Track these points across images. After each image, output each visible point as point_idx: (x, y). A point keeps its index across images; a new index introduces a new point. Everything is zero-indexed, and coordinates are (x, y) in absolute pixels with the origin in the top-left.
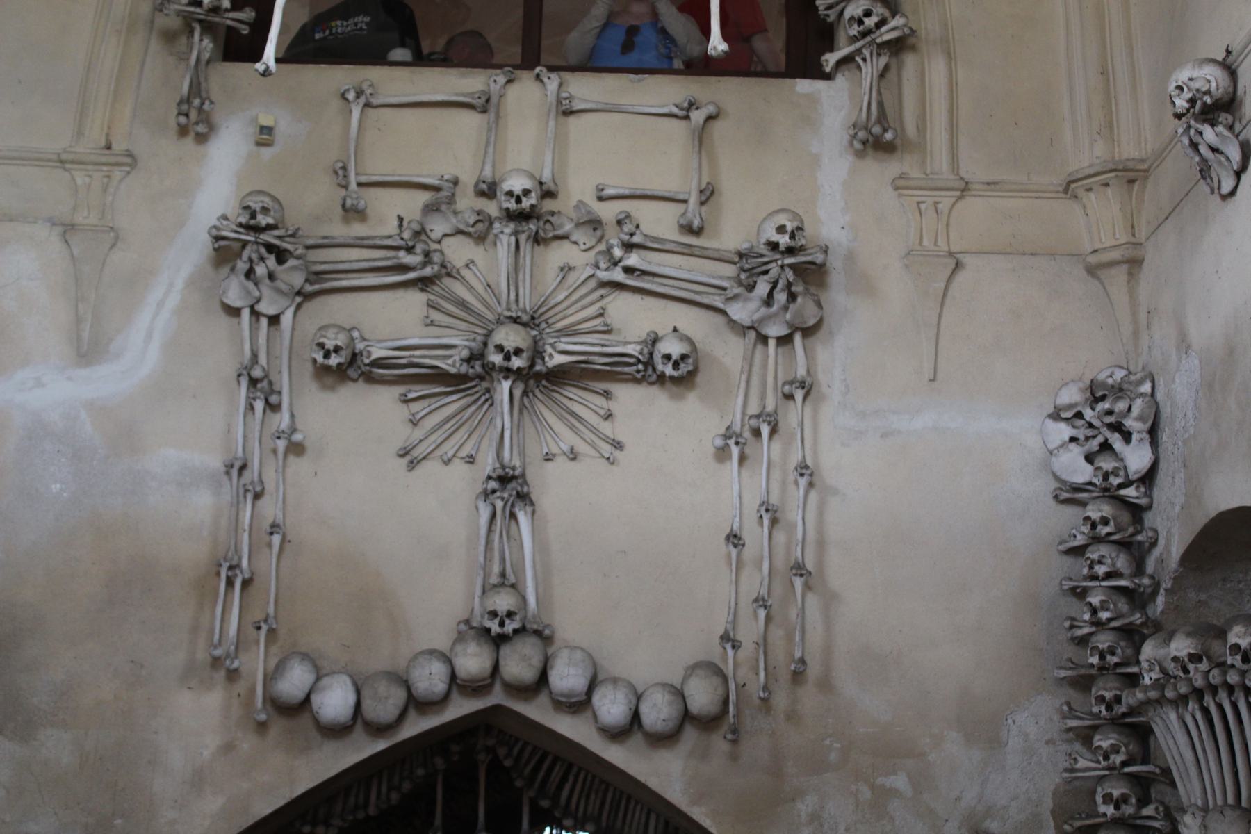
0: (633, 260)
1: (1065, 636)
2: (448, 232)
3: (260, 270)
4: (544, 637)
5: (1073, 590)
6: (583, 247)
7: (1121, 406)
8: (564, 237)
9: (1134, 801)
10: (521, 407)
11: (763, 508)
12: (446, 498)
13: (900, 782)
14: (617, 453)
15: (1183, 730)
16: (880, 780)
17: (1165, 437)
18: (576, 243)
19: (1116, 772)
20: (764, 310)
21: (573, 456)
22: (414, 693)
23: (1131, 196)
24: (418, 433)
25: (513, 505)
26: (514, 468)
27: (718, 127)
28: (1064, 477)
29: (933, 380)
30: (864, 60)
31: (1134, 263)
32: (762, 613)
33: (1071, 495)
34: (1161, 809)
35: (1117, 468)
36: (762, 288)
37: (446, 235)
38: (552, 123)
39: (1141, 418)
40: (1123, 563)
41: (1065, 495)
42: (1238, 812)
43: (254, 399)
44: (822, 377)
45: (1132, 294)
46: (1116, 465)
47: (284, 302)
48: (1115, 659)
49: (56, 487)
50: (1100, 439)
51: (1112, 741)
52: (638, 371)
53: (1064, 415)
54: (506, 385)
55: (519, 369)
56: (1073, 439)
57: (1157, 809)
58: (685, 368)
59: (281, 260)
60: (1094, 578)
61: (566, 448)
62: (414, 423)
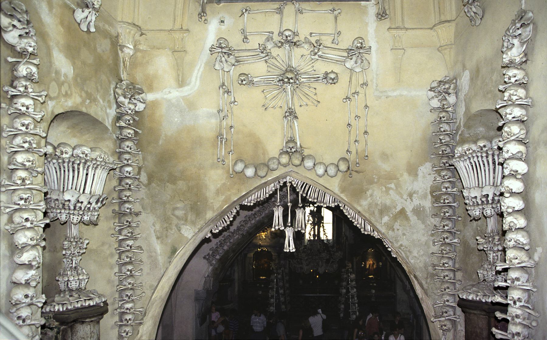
3: (223, 59)
16: (388, 185)
20: (355, 65)
44: (369, 83)
49: (176, 119)
54: (289, 87)
58: (335, 81)
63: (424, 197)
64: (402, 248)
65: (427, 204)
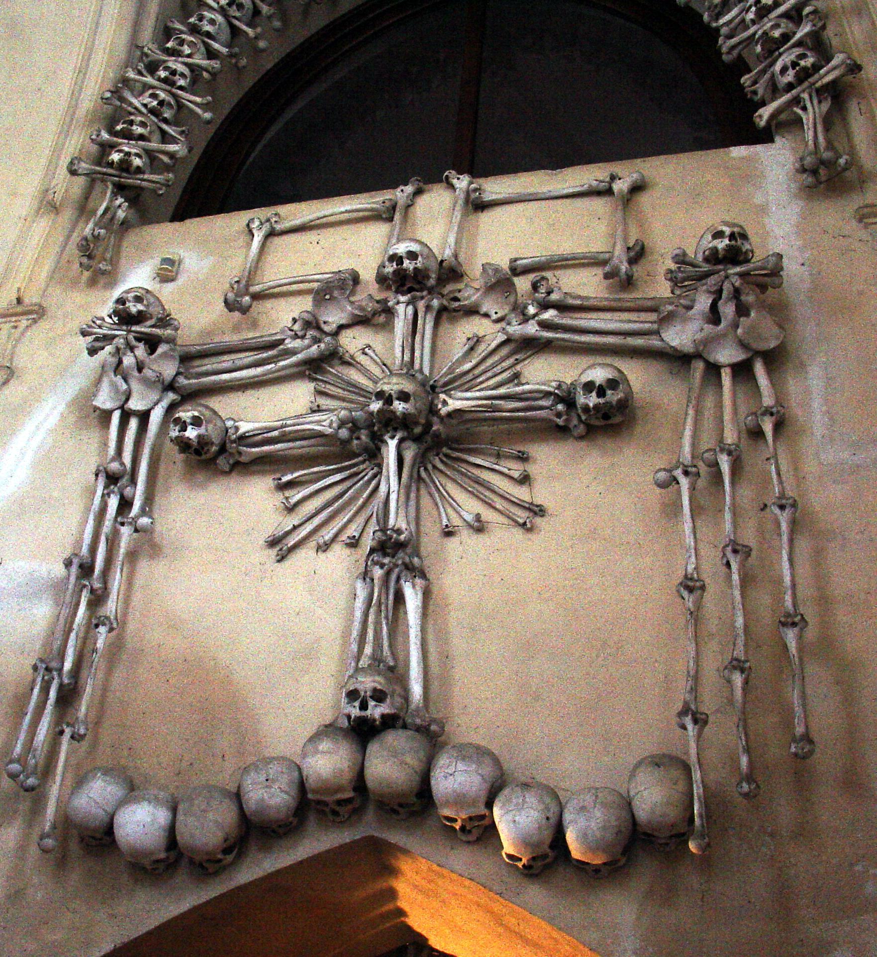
0: (549, 315)
2: (343, 322)
3: (128, 360)
4: (432, 738)
6: (494, 317)
8: (472, 311)
10: (416, 480)
11: (729, 548)
12: (323, 590)
14: (538, 520)
18: (486, 315)
20: (709, 328)
21: (479, 527)
22: (246, 810)
24: (295, 520)
25: (398, 579)
26: (399, 532)
27: (644, 200)
30: (804, 109)
32: (738, 679)
36: (703, 302)
37: (341, 327)
38: (458, 215)
43: (109, 495)
44: (795, 408)
47: (155, 396)
52: (559, 415)
54: (392, 444)
55: (405, 415)
59: (152, 349)
61: (469, 518)
62: (291, 509)
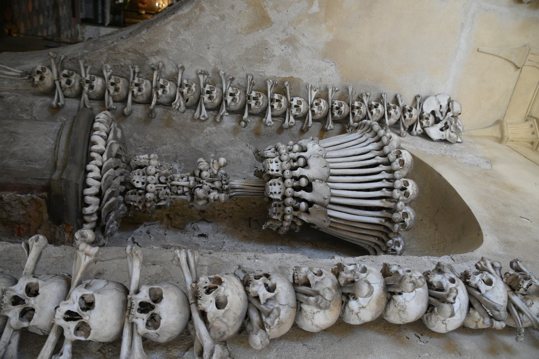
1: (362, 91)
5: (382, 97)
7: (452, 128)
9: (297, 114)
13: (315, 8)
15: (364, 151)
17: (445, 146)
19: (309, 108)
23: (526, 142)
28: (427, 101)
29: (478, 50)
31: (501, 140)
33: (418, 101)
34: (292, 124)
35: (429, 124)
39: (450, 136)
40: (393, 120)
41: (419, 100)
42: (327, 175)
45: (488, 137)
46: (430, 123)
48: (356, 113)
50: (441, 118)
51: (323, 108)
53: (450, 104)
56: (441, 106)
57: (292, 123)
60: (389, 108)
63: (285, 65)
64: (197, 11)
65: (272, 71)
